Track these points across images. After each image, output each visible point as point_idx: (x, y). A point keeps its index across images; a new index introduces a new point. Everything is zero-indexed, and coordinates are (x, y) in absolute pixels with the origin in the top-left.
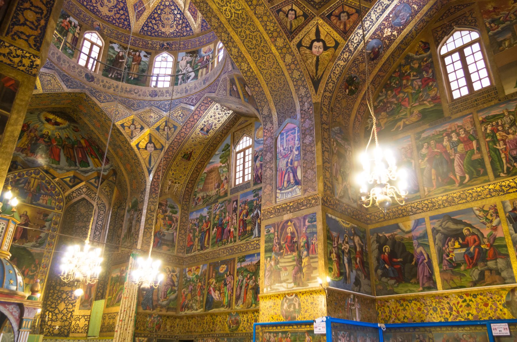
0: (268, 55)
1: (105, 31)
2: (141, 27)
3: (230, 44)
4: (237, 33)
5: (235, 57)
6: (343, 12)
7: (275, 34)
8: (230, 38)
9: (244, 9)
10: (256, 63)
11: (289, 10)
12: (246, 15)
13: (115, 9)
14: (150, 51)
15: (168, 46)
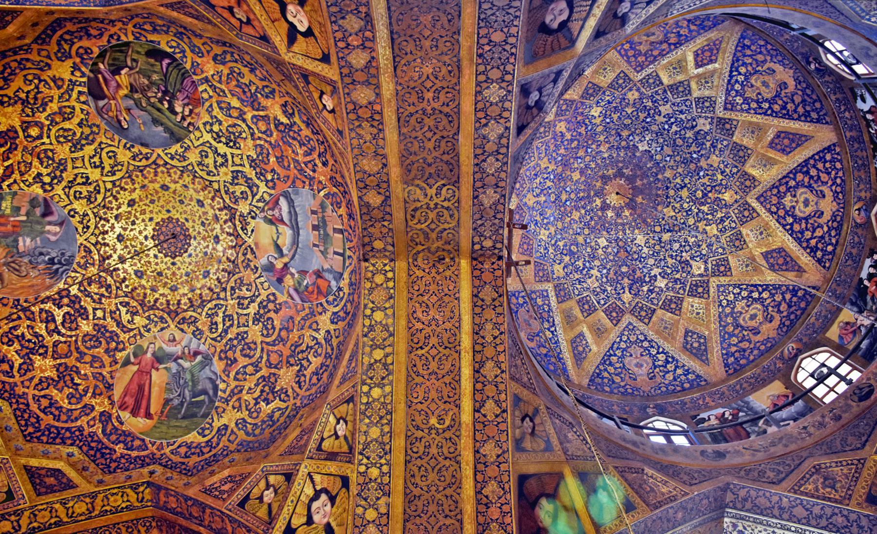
0: (412, 84)
1: (863, 194)
2: (818, 125)
3: (490, 147)
4: (457, 155)
5: (502, 121)
6: (239, 19)
7: (365, 113)
8: (482, 158)
9: (405, 183)
10: (458, 83)
11: (330, 112)
12: (410, 171)
13: (815, 185)
14: (849, 94)
15: (811, 59)
